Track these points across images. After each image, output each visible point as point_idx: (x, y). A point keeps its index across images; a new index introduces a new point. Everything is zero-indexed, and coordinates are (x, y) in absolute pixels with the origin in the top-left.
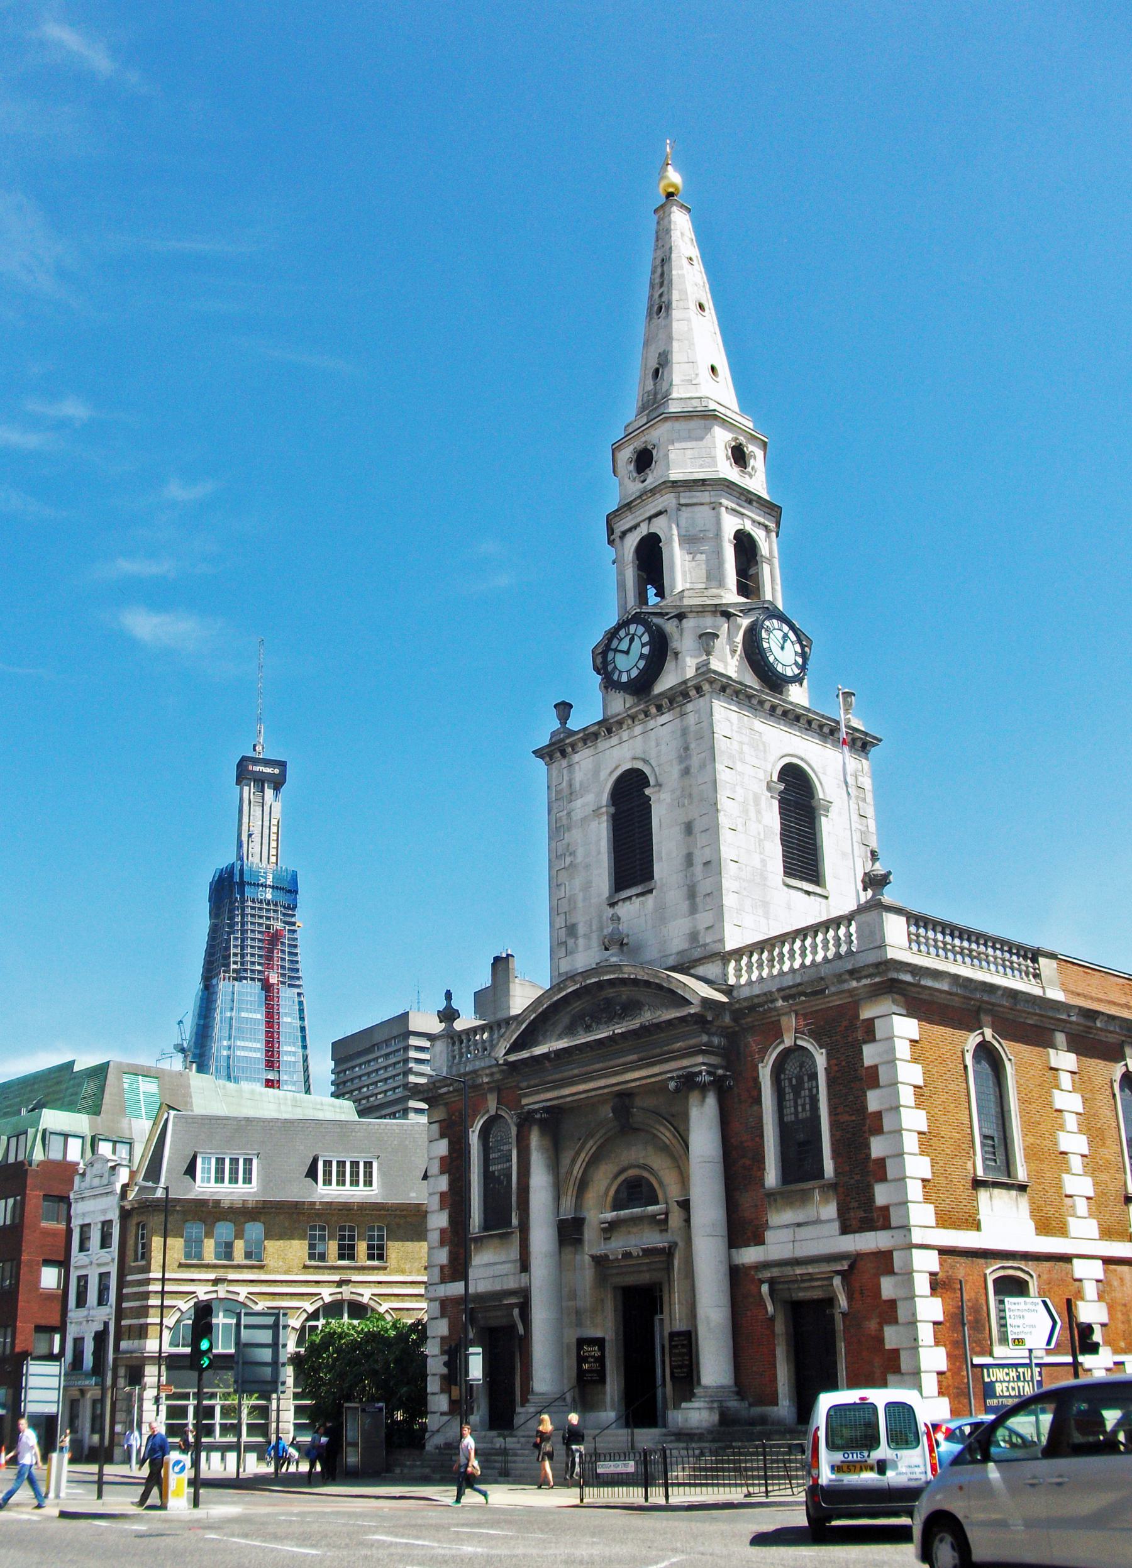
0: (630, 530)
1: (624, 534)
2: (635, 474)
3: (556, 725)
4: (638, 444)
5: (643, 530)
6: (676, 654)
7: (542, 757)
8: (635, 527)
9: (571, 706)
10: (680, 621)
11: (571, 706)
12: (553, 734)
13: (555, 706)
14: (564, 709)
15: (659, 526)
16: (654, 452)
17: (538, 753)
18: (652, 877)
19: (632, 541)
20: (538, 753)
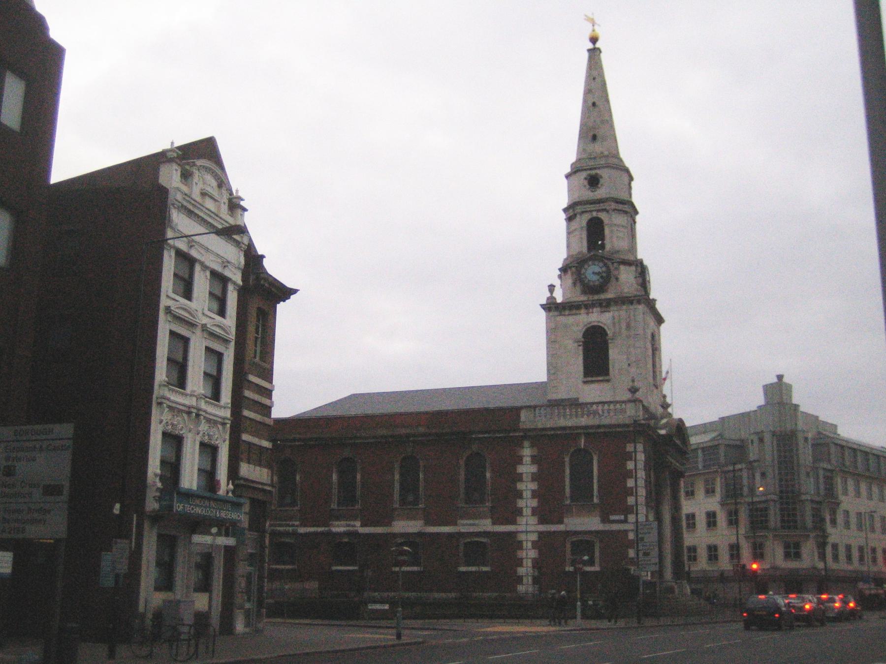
0: (586, 212)
1: (583, 212)
2: (588, 187)
3: (549, 295)
4: (593, 172)
5: (594, 214)
6: (617, 279)
7: (544, 309)
8: (591, 211)
9: (554, 286)
10: (619, 265)
11: (554, 286)
12: (548, 299)
13: (549, 286)
14: (551, 288)
15: (603, 216)
16: (601, 180)
17: (542, 306)
18: (607, 374)
19: (586, 218)
20: (542, 306)
